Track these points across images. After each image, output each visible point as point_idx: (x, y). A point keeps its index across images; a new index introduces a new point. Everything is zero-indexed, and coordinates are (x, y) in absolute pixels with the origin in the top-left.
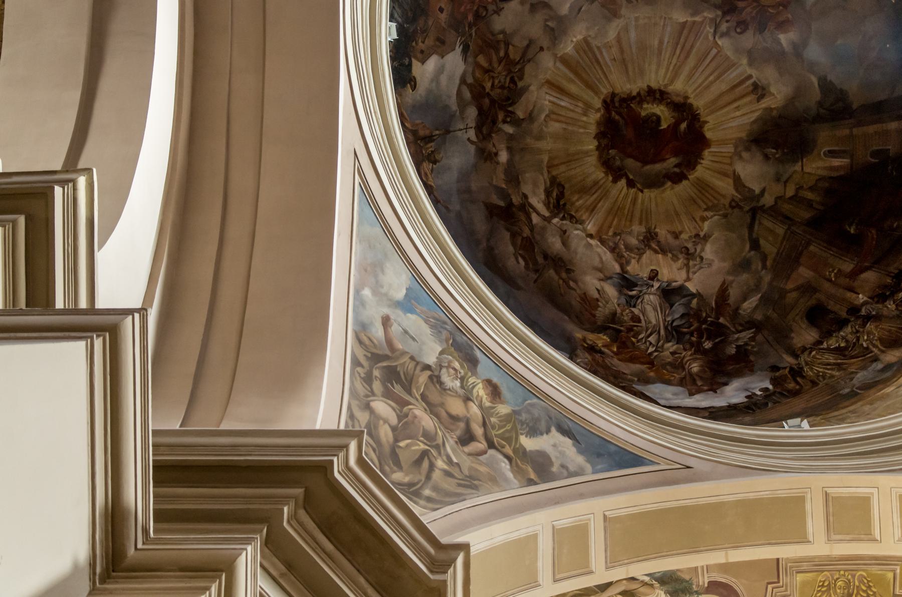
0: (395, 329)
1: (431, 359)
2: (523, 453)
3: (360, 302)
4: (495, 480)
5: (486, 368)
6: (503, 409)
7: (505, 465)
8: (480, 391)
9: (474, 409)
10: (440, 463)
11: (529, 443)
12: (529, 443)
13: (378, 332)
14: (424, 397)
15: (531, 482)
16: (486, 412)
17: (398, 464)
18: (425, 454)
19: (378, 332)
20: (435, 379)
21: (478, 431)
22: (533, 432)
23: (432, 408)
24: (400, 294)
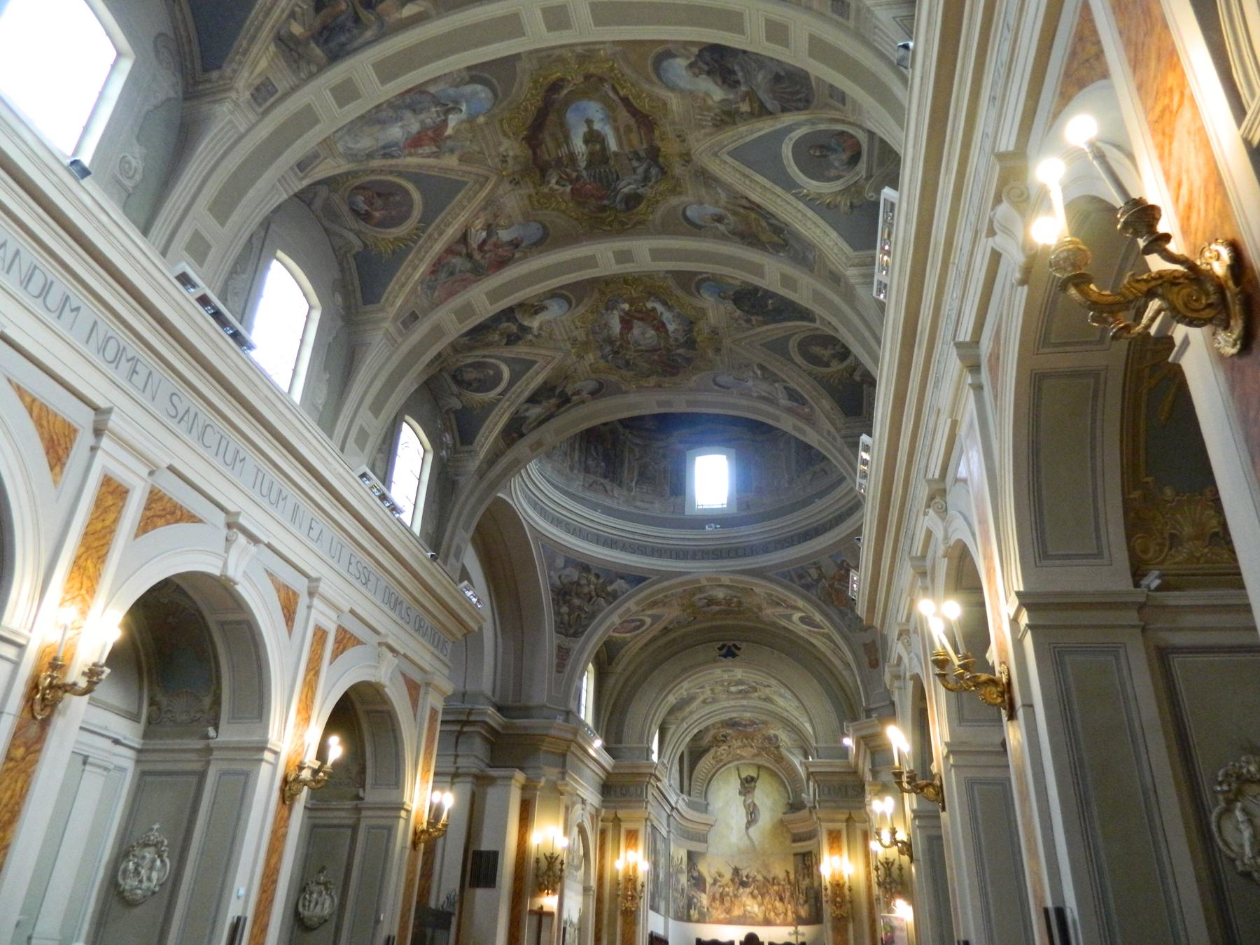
0: (563, 577)
1: (575, 579)
2: (608, 594)
3: (550, 577)
4: (600, 611)
5: (593, 572)
6: (601, 581)
7: (602, 601)
8: (593, 579)
9: (592, 587)
10: (583, 616)
11: (610, 589)
12: (610, 589)
13: (558, 582)
14: (577, 594)
15: (611, 603)
16: (595, 585)
17: (570, 625)
18: (579, 615)
19: (558, 582)
20: (578, 583)
21: (593, 593)
22: (611, 582)
23: (578, 595)
24: (562, 565)
